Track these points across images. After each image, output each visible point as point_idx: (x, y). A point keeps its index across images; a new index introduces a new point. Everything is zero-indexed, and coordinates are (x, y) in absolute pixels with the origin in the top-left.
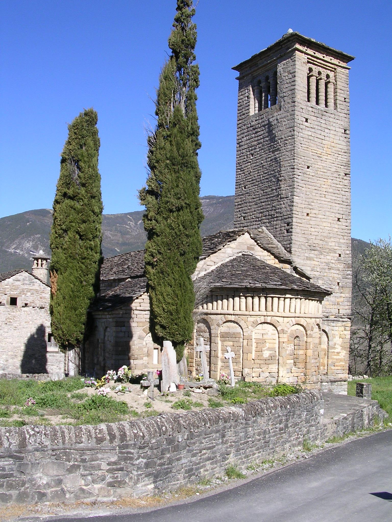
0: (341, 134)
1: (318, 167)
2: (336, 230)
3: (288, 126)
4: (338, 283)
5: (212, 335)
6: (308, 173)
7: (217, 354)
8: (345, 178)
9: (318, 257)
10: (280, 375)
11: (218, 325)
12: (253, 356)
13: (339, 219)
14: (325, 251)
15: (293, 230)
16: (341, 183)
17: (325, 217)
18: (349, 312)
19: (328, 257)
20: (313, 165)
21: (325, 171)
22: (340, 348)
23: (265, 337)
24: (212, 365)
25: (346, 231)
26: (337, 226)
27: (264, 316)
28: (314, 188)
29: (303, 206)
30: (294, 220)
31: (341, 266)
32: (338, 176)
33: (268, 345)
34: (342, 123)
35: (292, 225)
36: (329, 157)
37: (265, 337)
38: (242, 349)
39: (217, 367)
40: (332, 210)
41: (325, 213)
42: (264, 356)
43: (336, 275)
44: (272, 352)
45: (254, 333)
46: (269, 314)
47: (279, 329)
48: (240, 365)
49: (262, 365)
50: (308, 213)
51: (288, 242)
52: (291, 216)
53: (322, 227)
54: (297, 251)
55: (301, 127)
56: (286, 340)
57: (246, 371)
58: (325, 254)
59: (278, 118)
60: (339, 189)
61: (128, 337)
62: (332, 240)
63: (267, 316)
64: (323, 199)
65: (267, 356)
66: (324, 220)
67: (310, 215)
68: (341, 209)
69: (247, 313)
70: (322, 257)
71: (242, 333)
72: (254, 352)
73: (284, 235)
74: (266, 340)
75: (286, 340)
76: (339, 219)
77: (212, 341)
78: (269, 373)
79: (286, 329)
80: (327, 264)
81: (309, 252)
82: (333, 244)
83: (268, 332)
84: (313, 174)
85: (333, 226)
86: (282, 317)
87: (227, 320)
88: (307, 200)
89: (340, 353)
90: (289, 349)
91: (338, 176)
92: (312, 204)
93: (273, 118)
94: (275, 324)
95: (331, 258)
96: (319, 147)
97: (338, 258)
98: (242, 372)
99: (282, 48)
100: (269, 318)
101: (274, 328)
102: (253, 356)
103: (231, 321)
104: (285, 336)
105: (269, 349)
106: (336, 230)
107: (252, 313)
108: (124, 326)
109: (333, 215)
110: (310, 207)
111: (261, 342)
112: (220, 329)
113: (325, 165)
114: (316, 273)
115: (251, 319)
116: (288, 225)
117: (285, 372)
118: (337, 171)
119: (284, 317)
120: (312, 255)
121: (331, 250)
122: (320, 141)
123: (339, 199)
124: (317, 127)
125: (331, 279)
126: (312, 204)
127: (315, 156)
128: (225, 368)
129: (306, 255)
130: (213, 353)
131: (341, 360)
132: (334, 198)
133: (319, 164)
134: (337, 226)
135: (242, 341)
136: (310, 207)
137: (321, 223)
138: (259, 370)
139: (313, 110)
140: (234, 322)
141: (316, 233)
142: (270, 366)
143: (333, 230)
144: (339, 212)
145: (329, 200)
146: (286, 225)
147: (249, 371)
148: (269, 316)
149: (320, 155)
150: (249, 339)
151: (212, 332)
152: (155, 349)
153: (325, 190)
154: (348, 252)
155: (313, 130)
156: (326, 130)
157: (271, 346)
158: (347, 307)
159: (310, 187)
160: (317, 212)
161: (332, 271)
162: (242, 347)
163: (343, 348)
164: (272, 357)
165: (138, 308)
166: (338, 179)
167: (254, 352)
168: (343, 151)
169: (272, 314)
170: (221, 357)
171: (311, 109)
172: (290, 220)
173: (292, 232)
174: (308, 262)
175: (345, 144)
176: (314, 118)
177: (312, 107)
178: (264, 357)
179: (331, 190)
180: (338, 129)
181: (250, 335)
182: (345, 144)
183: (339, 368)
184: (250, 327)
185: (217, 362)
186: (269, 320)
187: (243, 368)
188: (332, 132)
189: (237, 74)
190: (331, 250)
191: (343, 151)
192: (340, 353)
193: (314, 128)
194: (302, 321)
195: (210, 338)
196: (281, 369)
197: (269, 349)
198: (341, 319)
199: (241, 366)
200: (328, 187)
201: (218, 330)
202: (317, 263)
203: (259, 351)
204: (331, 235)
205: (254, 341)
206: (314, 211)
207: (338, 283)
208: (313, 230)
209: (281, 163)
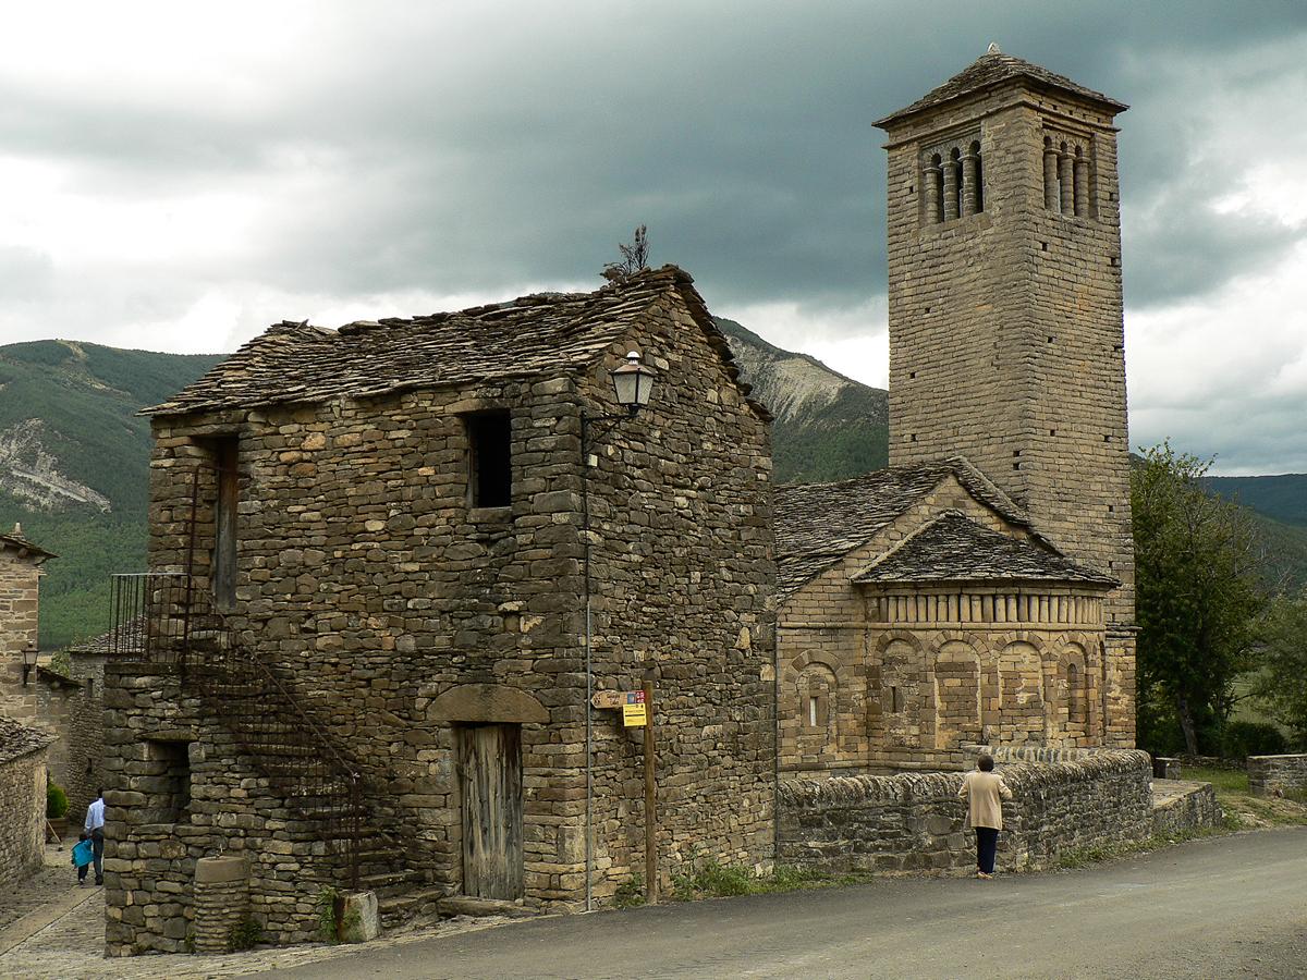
0: (1105, 268)
2: (1102, 459)
4: (1110, 563)
6: (1050, 351)
13: (1107, 437)
16: (1108, 366)
17: (1084, 436)
18: (1132, 617)
19: (1091, 514)
21: (1080, 344)
22: (1119, 689)
25: (1120, 460)
26: (1103, 452)
27: (1017, 630)
28: (1061, 379)
31: (1113, 530)
34: (1107, 245)
37: (1019, 667)
43: (1104, 547)
46: (1025, 625)
50: (1053, 428)
55: (1036, 260)
56: (1055, 672)
60: (1105, 378)
63: (1021, 630)
64: (1077, 400)
66: (1081, 441)
67: (1057, 433)
68: (1110, 418)
69: (986, 625)
72: (1001, 696)
76: (1107, 437)
80: (1090, 526)
82: (1099, 486)
84: (1059, 353)
85: (1097, 451)
88: (1051, 404)
89: (1119, 698)
92: (1060, 411)
93: (977, 241)
95: (1095, 514)
96: (1067, 298)
105: (1026, 689)
106: (1102, 459)
107: (994, 625)
110: (1056, 417)
111: (1012, 678)
113: (1079, 333)
114: (1071, 545)
115: (993, 637)
117: (1057, 729)
119: (1050, 631)
120: (1062, 511)
122: (1069, 285)
124: (1062, 258)
125: (1097, 555)
126: (1060, 411)
127: (1061, 316)
129: (1053, 511)
131: (1121, 713)
133: (1069, 331)
134: (1103, 452)
136: (1056, 417)
137: (1076, 449)
139: (1057, 225)
141: (1068, 468)
142: (1031, 720)
145: (1088, 401)
149: (1068, 314)
153: (1079, 381)
154: (1125, 501)
155: (1057, 265)
156: (1080, 263)
157: (1031, 683)
158: (1127, 610)
159: (1054, 378)
160: (1067, 426)
161: (1100, 540)
163: (1125, 689)
165: (784, 624)
166: (1103, 359)
167: (1001, 696)
168: (1110, 301)
169: (1031, 625)
171: (1050, 223)
174: (1056, 524)
176: (1058, 241)
177: (1053, 219)
180: (1099, 259)
183: (1120, 728)
188: (1090, 265)
189: (884, 137)
191: (1110, 301)
192: (1119, 698)
193: (1058, 261)
194: (1080, 638)
197: (1026, 689)
198: (1118, 633)
200: (1084, 375)
202: (1072, 526)
203: (1010, 693)
204: (1094, 470)
205: (1000, 675)
206: (1064, 426)
207: (1110, 563)
208: (1062, 462)
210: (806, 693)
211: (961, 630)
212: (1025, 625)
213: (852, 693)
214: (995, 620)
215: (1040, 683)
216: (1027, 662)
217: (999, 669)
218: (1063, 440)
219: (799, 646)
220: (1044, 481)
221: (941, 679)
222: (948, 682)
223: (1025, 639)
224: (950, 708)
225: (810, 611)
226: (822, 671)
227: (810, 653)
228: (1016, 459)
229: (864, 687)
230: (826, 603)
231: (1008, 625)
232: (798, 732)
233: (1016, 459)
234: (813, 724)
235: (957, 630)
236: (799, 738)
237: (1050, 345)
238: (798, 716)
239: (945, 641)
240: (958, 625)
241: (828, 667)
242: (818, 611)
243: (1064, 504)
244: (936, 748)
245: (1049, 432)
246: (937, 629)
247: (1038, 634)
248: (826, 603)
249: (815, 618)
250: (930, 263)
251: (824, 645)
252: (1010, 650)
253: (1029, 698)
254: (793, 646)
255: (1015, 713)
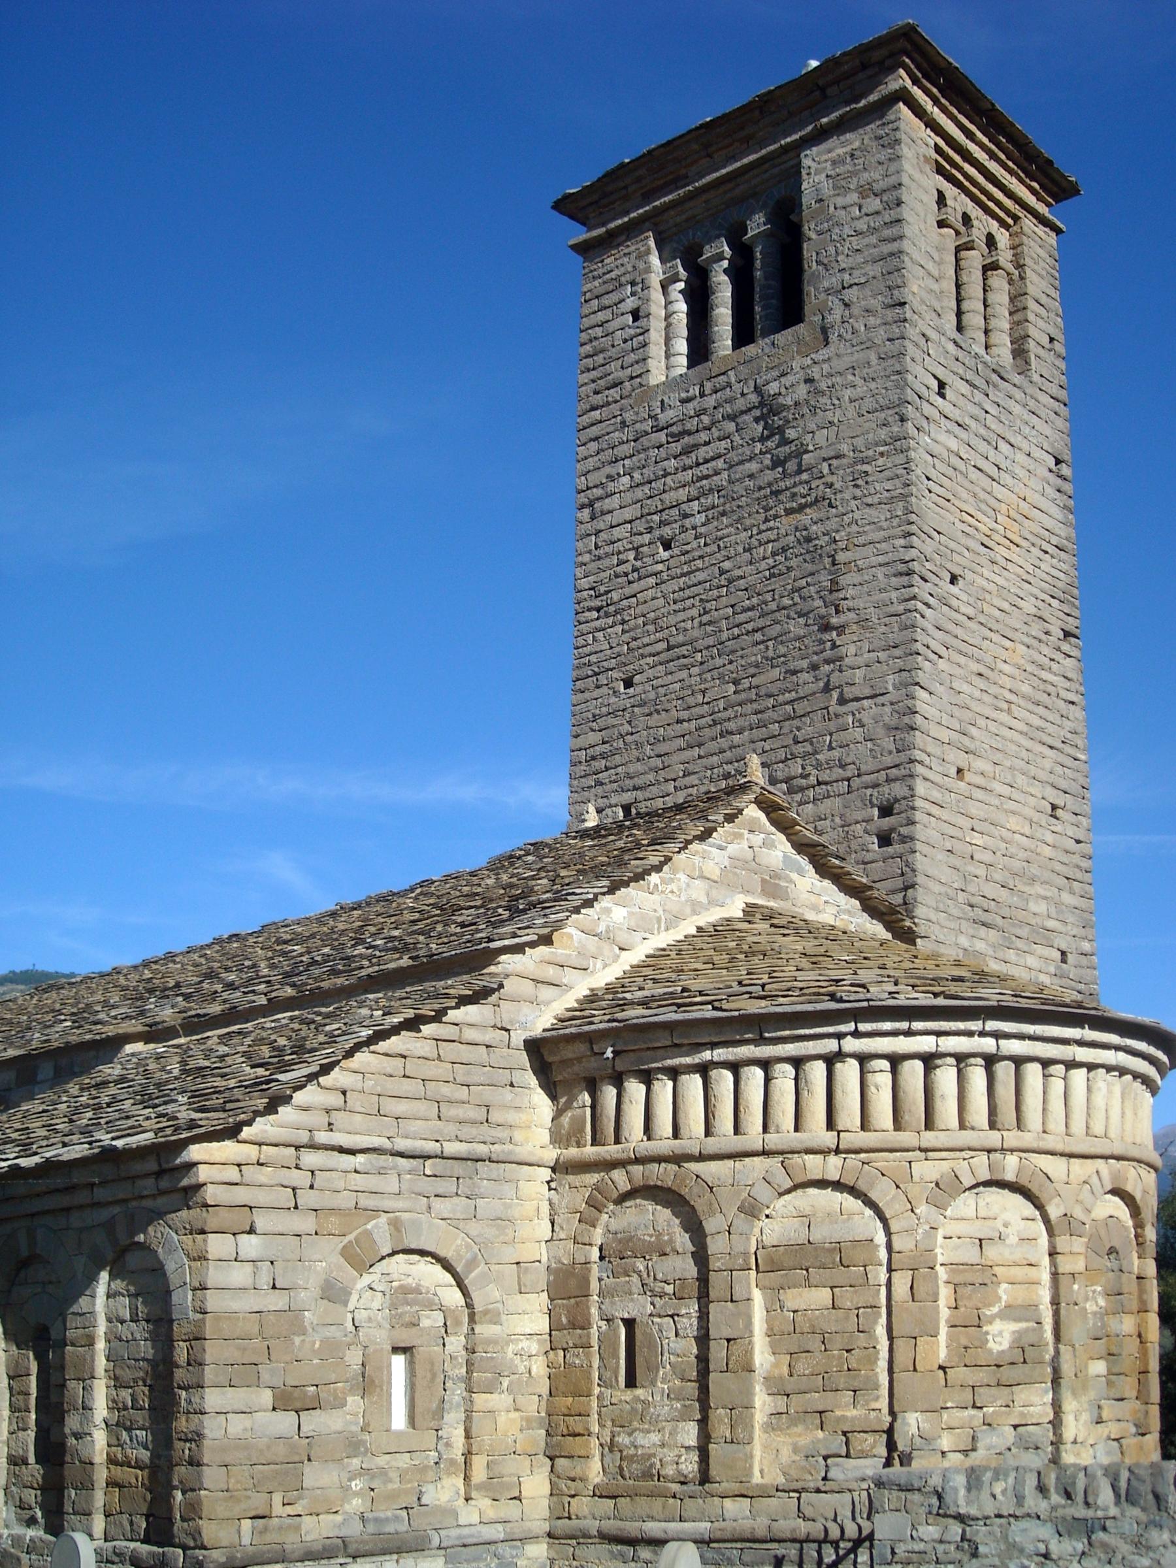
1: (985, 583)
3: (868, 403)
5: (715, 1264)
7: (749, 1352)
8: (1065, 647)
9: (1000, 955)
10: (1069, 1433)
11: (751, 1210)
12: (941, 1348)
13: (1054, 807)
14: (1019, 932)
15: (919, 831)
16: (1054, 666)
20: (969, 575)
23: (992, 1253)
24: (719, 1415)
25: (1076, 859)
28: (976, 667)
29: (945, 735)
30: (921, 788)
32: (1044, 637)
33: (1004, 1292)
35: (913, 808)
36: (1014, 554)
37: (992, 1253)
38: (883, 1320)
39: (752, 1415)
40: (1033, 771)
41: (1014, 776)
42: (991, 1345)
44: (1024, 1325)
45: (940, 1233)
46: (1012, 1138)
47: (1054, 1212)
48: (877, 1398)
49: (983, 1395)
51: (898, 882)
52: (907, 772)
53: (1004, 833)
54: (934, 919)
56: (1079, 1265)
57: (912, 1423)
58: (1019, 944)
59: (815, 372)
60: (1050, 689)
61: (274, 1287)
62: (1039, 889)
63: (1003, 1150)
64: (1004, 717)
65: (1005, 1346)
66: (1011, 805)
67: (968, 776)
68: (1059, 769)
69: (906, 1138)
70: (1011, 955)
71: (880, 1238)
72: (943, 1330)
73: (869, 857)
74: (996, 1270)
75: (1079, 1265)
77: (713, 1294)
78: (1015, 1427)
79: (1078, 1213)
81: (971, 932)
83: (1002, 1229)
84: (970, 611)
86: (1062, 1155)
87: (800, 1179)
88: (957, 712)
90: (1090, 1307)
91: (1044, 637)
92: (973, 731)
94: (1034, 1188)
96: (983, 507)
97: (1057, 968)
98: (890, 1432)
99: (825, 97)
100: (1012, 1161)
101: (1029, 1210)
102: (941, 1348)
103: (822, 1184)
104: (1079, 1244)
105: (1010, 1312)
108: (252, 1231)
109: (1036, 789)
110: (966, 741)
112: (757, 1231)
113: (1006, 584)
115: (928, 1170)
116: (886, 811)
118: (1039, 614)
119: (1071, 1156)
121: (1038, 933)
123: (1051, 728)
128: (794, 1422)
130: (718, 1352)
132: (1037, 722)
134: (1049, 838)
135: (883, 1277)
136: (966, 741)
137: (1000, 817)
138: (972, 1417)
140: (838, 1186)
141: (987, 857)
142: (1022, 1395)
143: (1039, 850)
144: (1052, 778)
146: (876, 812)
147: (925, 1426)
148: (1012, 1151)
150: (921, 1265)
151: (716, 1246)
152: (396, 1350)
156: (1003, 446)
157: (1021, 1295)
159: (962, 660)
162: (884, 1310)
164: (1023, 1353)
165: (322, 1137)
167: (943, 1330)
169: (1027, 1139)
170: (767, 1366)
172: (899, 790)
173: (912, 839)
175: (1060, 517)
178: (990, 1351)
179: (1025, 688)
181: (922, 1247)
182: (1060, 517)
184: (922, 1209)
185: (750, 1394)
186: (1010, 1167)
187: (892, 1413)
190: (1038, 933)
191: (1055, 540)
195: (703, 1280)
196: (1070, 1405)
199: (883, 1404)
200: (1016, 672)
201: (746, 1236)
204: (1034, 870)
205: (941, 1272)
206: (980, 764)
208: (978, 839)
209: (841, 557)
210: (381, 1338)
211: (837, 1151)
212: (1012, 1138)
213: (511, 1337)
214: (929, 1124)
215: (1045, 1295)
216: (1013, 1239)
217: (940, 1259)
218: (979, 794)
219: (366, 1201)
220: (946, 875)
221: (774, 1292)
222: (798, 1298)
223: (1010, 1176)
224: (802, 1367)
225: (401, 1108)
226: (429, 1274)
227: (396, 1225)
228: (887, 822)
229: (543, 1324)
230: (446, 1090)
231: (967, 1138)
232: (354, 1446)
233: (887, 822)
234: (399, 1420)
235: (823, 1152)
236: (356, 1462)
237: (954, 589)
238: (354, 1402)
239: (788, 1184)
240: (829, 1139)
241: (447, 1266)
242: (421, 1108)
243: (983, 931)
244: (757, 1479)
245: (953, 771)
246: (765, 1153)
247: (1044, 1162)
248: (446, 1090)
249: (415, 1126)
250: (676, 447)
251: (437, 1203)
252: (965, 1205)
253: (1018, 1336)
254: (346, 1201)
255: (981, 1376)
